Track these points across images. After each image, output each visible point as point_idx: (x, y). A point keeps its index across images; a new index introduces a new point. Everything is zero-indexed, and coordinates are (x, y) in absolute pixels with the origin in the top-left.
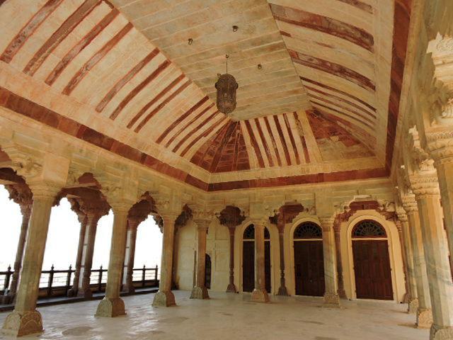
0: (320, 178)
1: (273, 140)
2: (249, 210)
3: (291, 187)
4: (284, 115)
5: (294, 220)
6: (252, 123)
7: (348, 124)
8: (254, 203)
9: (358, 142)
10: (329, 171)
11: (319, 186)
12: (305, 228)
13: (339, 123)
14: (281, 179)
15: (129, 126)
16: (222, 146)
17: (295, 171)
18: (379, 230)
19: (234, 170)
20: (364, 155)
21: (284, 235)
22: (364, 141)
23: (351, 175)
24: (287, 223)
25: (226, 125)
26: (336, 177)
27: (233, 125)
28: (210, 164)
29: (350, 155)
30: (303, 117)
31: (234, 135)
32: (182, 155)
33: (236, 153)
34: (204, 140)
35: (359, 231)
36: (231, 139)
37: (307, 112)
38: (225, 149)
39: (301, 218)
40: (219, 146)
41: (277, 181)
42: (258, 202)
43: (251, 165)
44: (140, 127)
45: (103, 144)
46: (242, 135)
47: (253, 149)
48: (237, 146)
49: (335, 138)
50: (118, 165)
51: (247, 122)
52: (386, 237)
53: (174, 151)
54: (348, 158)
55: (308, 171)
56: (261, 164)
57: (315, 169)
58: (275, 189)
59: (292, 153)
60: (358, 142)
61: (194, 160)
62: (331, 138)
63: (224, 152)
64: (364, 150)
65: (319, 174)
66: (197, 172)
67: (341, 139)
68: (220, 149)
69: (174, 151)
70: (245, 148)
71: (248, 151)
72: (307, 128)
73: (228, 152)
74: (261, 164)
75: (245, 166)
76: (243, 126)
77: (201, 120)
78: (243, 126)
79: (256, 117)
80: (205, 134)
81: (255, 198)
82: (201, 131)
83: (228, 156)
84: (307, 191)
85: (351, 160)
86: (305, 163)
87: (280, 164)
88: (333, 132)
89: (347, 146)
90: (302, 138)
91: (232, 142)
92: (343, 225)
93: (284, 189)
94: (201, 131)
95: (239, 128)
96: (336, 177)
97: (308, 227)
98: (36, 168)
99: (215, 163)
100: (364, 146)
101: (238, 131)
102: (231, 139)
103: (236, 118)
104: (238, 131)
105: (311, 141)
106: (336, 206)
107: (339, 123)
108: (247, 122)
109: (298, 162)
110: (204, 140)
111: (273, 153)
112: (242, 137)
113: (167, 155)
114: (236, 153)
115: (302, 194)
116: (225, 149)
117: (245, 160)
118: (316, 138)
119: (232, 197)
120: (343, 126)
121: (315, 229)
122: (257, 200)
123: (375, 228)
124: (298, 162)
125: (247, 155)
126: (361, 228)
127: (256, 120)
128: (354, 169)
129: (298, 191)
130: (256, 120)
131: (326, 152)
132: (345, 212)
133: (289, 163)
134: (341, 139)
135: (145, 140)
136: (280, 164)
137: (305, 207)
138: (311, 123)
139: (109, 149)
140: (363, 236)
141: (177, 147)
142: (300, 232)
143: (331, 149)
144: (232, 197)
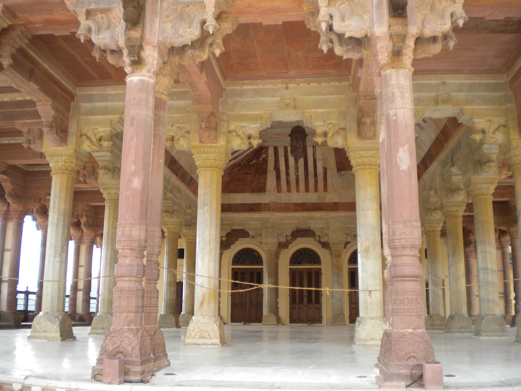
2: (261, 235)
3: (305, 214)
4: (313, 147)
5: (290, 246)
10: (344, 201)
11: (333, 214)
12: (302, 254)
14: (295, 204)
17: (312, 198)
18: (314, 258)
19: (248, 192)
24: (283, 248)
36: (254, 161)
47: (274, 172)
51: (276, 149)
58: (290, 214)
65: (334, 203)
75: (261, 189)
76: (271, 151)
78: (271, 151)
79: (287, 145)
87: (298, 191)
90: (325, 169)
91: (253, 165)
93: (298, 214)
95: (267, 153)
97: (299, 256)
104: (264, 156)
106: (347, 234)
108: (276, 149)
109: (316, 190)
112: (265, 161)
115: (315, 220)
118: (338, 171)
122: (269, 225)
124: (316, 190)
125: (266, 178)
129: (313, 218)
133: (307, 190)
136: (298, 191)
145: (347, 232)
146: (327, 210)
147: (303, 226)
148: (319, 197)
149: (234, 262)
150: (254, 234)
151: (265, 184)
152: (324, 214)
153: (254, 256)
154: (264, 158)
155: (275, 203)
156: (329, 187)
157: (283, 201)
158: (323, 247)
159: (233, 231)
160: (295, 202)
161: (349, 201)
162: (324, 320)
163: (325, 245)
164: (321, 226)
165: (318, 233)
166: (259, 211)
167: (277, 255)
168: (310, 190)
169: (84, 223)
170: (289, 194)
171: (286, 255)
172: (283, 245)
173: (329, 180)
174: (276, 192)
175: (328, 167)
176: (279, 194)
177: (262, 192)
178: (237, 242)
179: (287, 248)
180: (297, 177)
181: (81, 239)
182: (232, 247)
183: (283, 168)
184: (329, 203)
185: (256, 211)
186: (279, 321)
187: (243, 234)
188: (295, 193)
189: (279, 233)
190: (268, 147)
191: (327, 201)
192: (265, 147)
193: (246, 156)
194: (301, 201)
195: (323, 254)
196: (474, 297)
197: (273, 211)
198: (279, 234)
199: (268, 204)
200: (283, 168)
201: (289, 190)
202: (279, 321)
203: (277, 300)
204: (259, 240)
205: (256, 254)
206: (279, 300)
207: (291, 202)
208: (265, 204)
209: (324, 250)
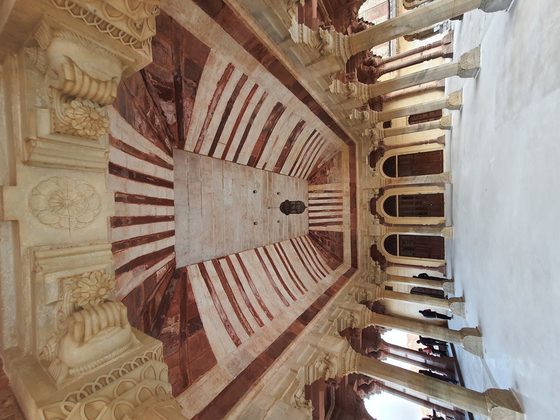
0: (353, 185)
1: (325, 211)
6: (311, 221)
7: (320, 160)
8: (368, 232)
9: (332, 160)
10: (349, 179)
11: (358, 186)
13: (319, 167)
17: (346, 201)
20: (340, 158)
21: (393, 223)
22: (331, 155)
23: (352, 167)
26: (353, 176)
27: (311, 234)
29: (339, 166)
30: (312, 188)
31: (318, 237)
32: (328, 273)
33: (330, 239)
34: (318, 256)
36: (320, 240)
37: (309, 185)
38: (327, 247)
41: (353, 214)
42: (368, 230)
45: (314, 313)
46: (319, 231)
48: (326, 237)
49: (328, 172)
50: (331, 310)
51: (310, 225)
52: (395, 156)
53: (325, 276)
54: (341, 167)
55: (347, 192)
56: (340, 223)
57: (346, 187)
58: (358, 216)
59: (334, 201)
60: (332, 160)
63: (329, 248)
64: (337, 157)
66: (342, 270)
67: (329, 169)
68: (326, 250)
69: (325, 276)
70: (327, 232)
72: (319, 187)
73: (329, 245)
74: (340, 223)
75: (341, 234)
76: (312, 228)
77: (305, 251)
78: (312, 228)
80: (315, 254)
81: (365, 231)
82: (312, 254)
84: (361, 194)
85: (342, 165)
87: (341, 210)
88: (324, 172)
89: (333, 166)
90: (325, 192)
91: (322, 240)
92: (386, 220)
93: (358, 210)
94: (312, 254)
95: (313, 231)
96: (353, 176)
98: (330, 358)
99: (336, 257)
100: (334, 157)
101: (316, 233)
102: (320, 240)
103: (307, 232)
104: (316, 233)
105: (328, 187)
107: (319, 167)
108: (310, 225)
109: (341, 198)
110: (318, 256)
111: (333, 214)
113: (329, 280)
114: (330, 239)
115: (363, 197)
116: (327, 247)
117: (336, 235)
118: (326, 183)
119: (363, 250)
120: (321, 164)
122: (366, 230)
127: (310, 218)
129: (362, 200)
130: (310, 218)
131: (336, 178)
133: (341, 204)
134: (329, 169)
136: (341, 210)
137: (374, 243)
138: (316, 184)
139: (318, 311)
143: (334, 176)
144: (363, 250)
147: (368, 207)
151: (337, 232)
159: (372, 255)
162: (441, 192)
163: (382, 191)
165: (372, 196)
169: (365, 381)
171: (389, 219)
172: (382, 221)
181: (380, 384)
186: (442, 226)
187: (374, 248)
191: (349, 190)
195: (388, 193)
201: (340, 216)
202: (442, 226)
203: (424, 226)
204: (378, 238)
206: (424, 224)
208: (351, 233)
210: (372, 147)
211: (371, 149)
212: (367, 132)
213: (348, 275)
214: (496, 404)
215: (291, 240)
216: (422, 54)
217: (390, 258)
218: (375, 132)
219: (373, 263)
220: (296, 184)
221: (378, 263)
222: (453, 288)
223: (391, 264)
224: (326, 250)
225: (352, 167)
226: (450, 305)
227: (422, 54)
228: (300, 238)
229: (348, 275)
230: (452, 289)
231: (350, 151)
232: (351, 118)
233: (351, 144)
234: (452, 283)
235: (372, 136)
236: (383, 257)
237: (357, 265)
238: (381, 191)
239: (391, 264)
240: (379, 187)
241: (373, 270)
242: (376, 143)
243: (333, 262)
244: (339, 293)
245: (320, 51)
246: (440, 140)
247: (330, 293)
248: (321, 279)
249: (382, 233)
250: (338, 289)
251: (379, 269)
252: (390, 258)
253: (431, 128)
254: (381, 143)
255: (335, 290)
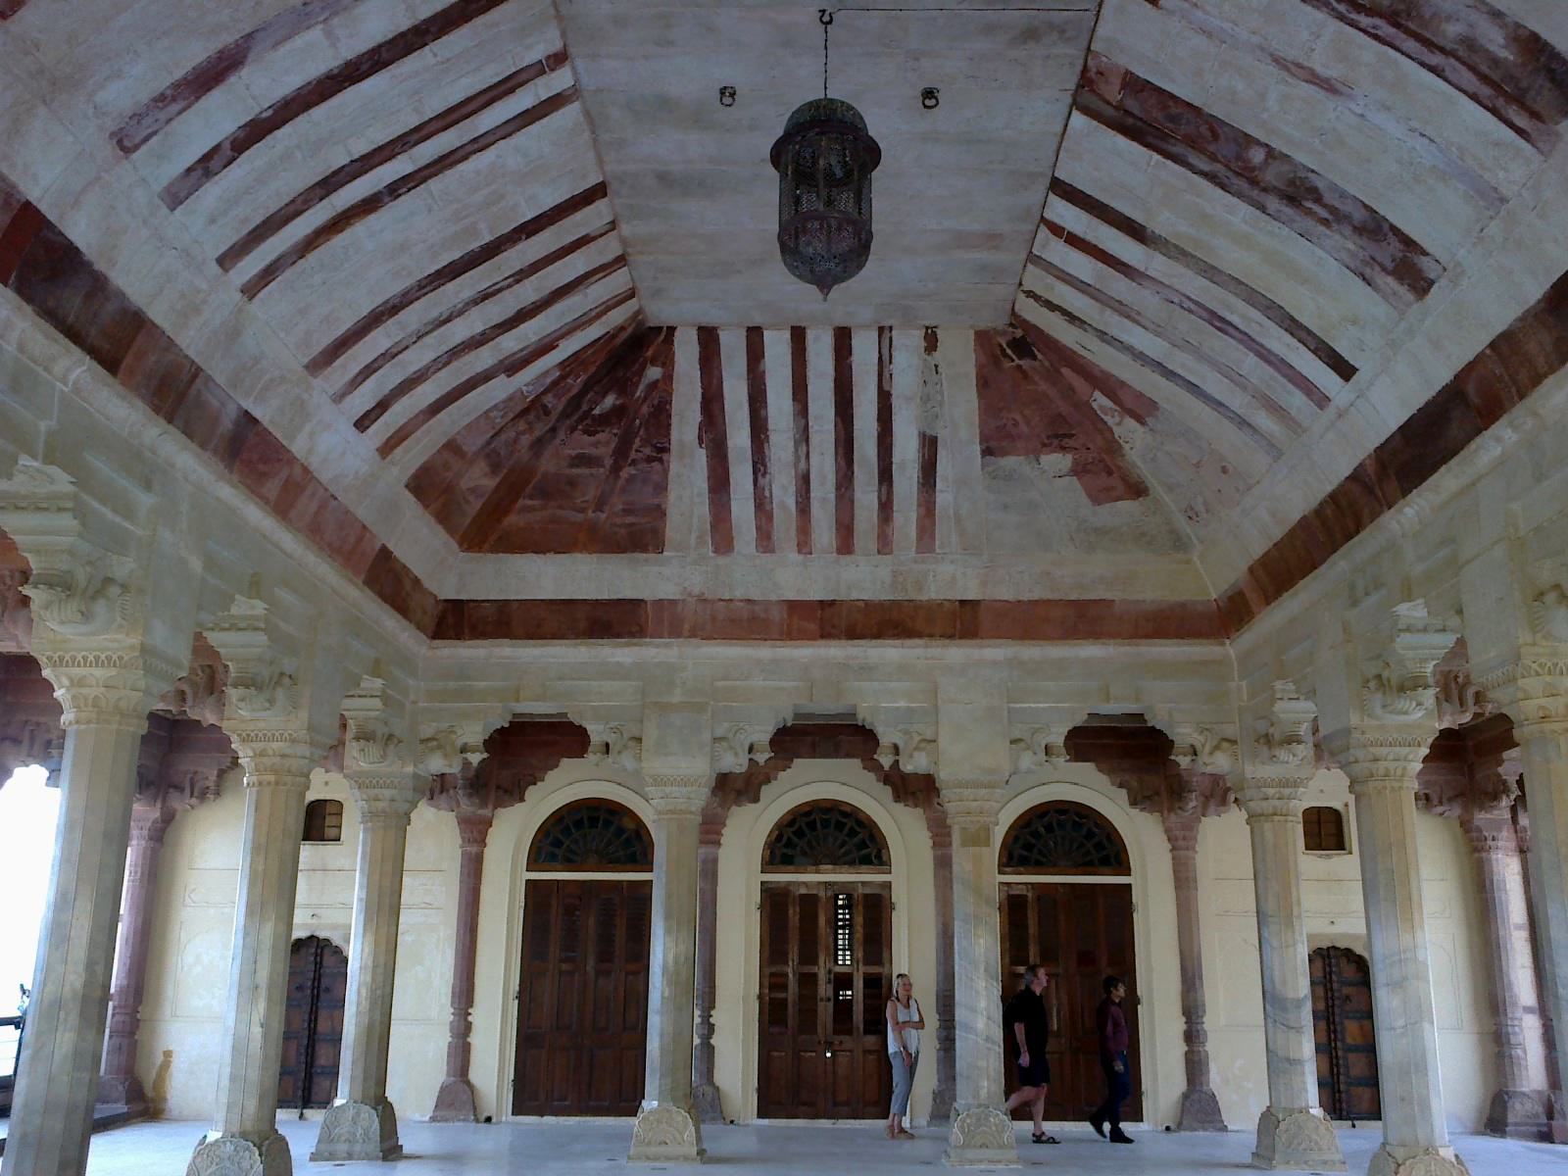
0: (964, 620)
1: (804, 435)
2: (639, 740)
3: (836, 651)
4: (881, 330)
5: (765, 791)
8: (664, 708)
10: (1005, 593)
11: (956, 653)
14: (793, 606)
15: (228, 259)
16: (553, 430)
17: (863, 578)
23: (1083, 619)
24: (738, 802)
25: (609, 337)
26: (1027, 621)
28: (475, 506)
30: (960, 356)
31: (624, 387)
32: (386, 449)
33: (616, 469)
34: (500, 389)
35: (1028, 847)
36: (610, 401)
39: (563, 786)
40: (540, 429)
41: (776, 614)
43: (672, 529)
44: (268, 274)
47: (701, 456)
49: (1057, 461)
51: (708, 338)
52: (1127, 872)
53: (362, 424)
57: (950, 578)
58: (765, 652)
61: (426, 486)
62: (1044, 458)
65: (963, 602)
69: (362, 424)
71: (675, 466)
76: (686, 353)
78: (686, 353)
79: (757, 320)
80: (512, 366)
83: (572, 483)
86: (913, 553)
87: (804, 545)
88: (1058, 436)
90: (930, 445)
91: (604, 420)
95: (666, 360)
96: (1027, 621)
99: (498, 506)
102: (610, 401)
103: (660, 313)
104: (654, 373)
106: (1013, 742)
108: (708, 338)
109: (885, 545)
110: (500, 389)
111: (782, 491)
113: (333, 446)
114: (616, 469)
115: (879, 680)
118: (987, 452)
121: (852, 833)
122: (677, 696)
123: (1090, 835)
124: (885, 545)
125: (662, 488)
126: (1036, 834)
127: (755, 335)
128: (1108, 596)
129: (866, 670)
130: (755, 335)
132: (467, 764)
133: (846, 542)
135: (261, 342)
136: (804, 545)
138: (984, 384)
140: (1039, 866)
141: (382, 406)
142: (789, 844)
145: (1017, 735)
146: (931, 636)
147: (825, 705)
148: (895, 574)
149: (536, 860)
150: (611, 738)
152: (920, 651)
153: (621, 831)
154: (654, 385)
155: (703, 600)
156: (943, 529)
157: (739, 594)
158: (897, 798)
160: (791, 596)
161: (1026, 596)
163: (915, 789)
164: (902, 704)
165: (887, 736)
166: (632, 635)
167: (711, 830)
168: (859, 541)
170: (767, 558)
171: (749, 830)
172: (735, 789)
173: (944, 497)
174: (708, 549)
175: (943, 434)
176: (722, 560)
177: (644, 549)
178: (551, 775)
179: (756, 799)
180: (804, 481)
182: (532, 793)
183: (739, 438)
184: (940, 604)
185: (619, 636)
187: (562, 738)
188: (794, 556)
189: (719, 733)
190: (672, 330)
192: (660, 329)
193: (569, 366)
194: (816, 594)
195: (902, 829)
196: (1519, 1013)
197: (693, 635)
198: (716, 740)
199: (673, 602)
200: (739, 438)
201: (765, 539)
204: (627, 761)
205: (630, 825)
206: (717, 1017)
207: (774, 597)
209: (900, 808)
210: (1197, 739)
211: (1183, 733)
212: (1295, 711)
213: (387, 578)
214: (264, 1149)
215: (598, 192)
216: (1528, 1010)
217: (513, 830)
218: (1294, 760)
219: (474, 733)
220: (992, 240)
221: (475, 758)
222: (350, 1157)
223: (476, 833)
224: (539, 445)
225: (1083, 619)
226: (244, 1135)
227: (1528, 1010)
228: (621, 261)
229: (387, 578)
230: (342, 1147)
231: (1183, 605)
232: (1403, 609)
233: (1230, 616)
234: (374, 1146)
235: (1271, 741)
236: (513, 792)
237: (458, 636)
238: (915, 789)
239: (476, 833)
240: (943, 775)
241: (427, 731)
242: (1220, 763)
243: (465, 483)
244: (255, 515)
245: (1557, 587)
246: (1199, 1107)
247: (249, 450)
248: (339, 397)
249: (660, 786)
250: (282, 509)
251: (437, 764)
252: (513, 830)
253: (1278, 1065)
254: (1220, 793)
255: (272, 488)
